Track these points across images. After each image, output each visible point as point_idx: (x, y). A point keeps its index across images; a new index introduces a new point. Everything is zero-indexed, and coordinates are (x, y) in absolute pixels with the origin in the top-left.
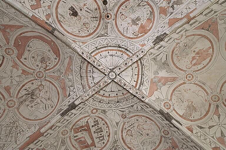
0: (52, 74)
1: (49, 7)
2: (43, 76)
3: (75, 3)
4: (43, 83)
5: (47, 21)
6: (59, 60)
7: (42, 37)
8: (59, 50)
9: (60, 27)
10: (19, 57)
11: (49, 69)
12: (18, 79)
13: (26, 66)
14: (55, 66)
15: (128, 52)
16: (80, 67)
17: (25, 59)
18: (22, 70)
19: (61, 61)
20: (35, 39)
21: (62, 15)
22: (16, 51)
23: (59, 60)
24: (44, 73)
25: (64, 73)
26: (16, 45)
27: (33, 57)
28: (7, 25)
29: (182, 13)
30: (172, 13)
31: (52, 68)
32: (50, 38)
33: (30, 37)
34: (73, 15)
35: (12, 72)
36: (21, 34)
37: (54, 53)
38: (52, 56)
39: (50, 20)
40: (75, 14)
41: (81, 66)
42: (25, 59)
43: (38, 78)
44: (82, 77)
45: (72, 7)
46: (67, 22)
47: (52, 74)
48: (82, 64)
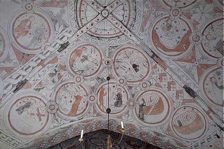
0: (163, 12)
1: (153, 73)
2: (173, 11)
3: (133, 74)
4: (174, 3)
5: (157, 64)
6: (154, 27)
7: (164, 50)
8: (152, 37)
9: (148, 58)
10: (190, 32)
11: (166, 18)
12: (197, 10)
13: (186, 23)
14: (160, 21)
15: (91, 34)
16: (135, 20)
17: (185, 30)
18: (191, 19)
19: (152, 25)
20: (171, 49)
21: (145, 66)
22: (191, 38)
23: (154, 27)
24: (171, 14)
25: (152, 13)
26: (188, 43)
27: (177, 31)
28: (189, 62)
29: (48, 68)
30: (56, 66)
31: (163, 19)
32: (158, 49)
33: (174, 51)
34: (136, 66)
35: (201, 19)
36: (180, 54)
37: (157, 35)
38: (160, 32)
39: (154, 64)
40: (135, 66)
41: (134, 21)
42: (185, 30)
43: (178, 9)
44: (135, 10)
45: (136, 72)
46: (142, 61)
47: (163, 12)
48: (133, 24)
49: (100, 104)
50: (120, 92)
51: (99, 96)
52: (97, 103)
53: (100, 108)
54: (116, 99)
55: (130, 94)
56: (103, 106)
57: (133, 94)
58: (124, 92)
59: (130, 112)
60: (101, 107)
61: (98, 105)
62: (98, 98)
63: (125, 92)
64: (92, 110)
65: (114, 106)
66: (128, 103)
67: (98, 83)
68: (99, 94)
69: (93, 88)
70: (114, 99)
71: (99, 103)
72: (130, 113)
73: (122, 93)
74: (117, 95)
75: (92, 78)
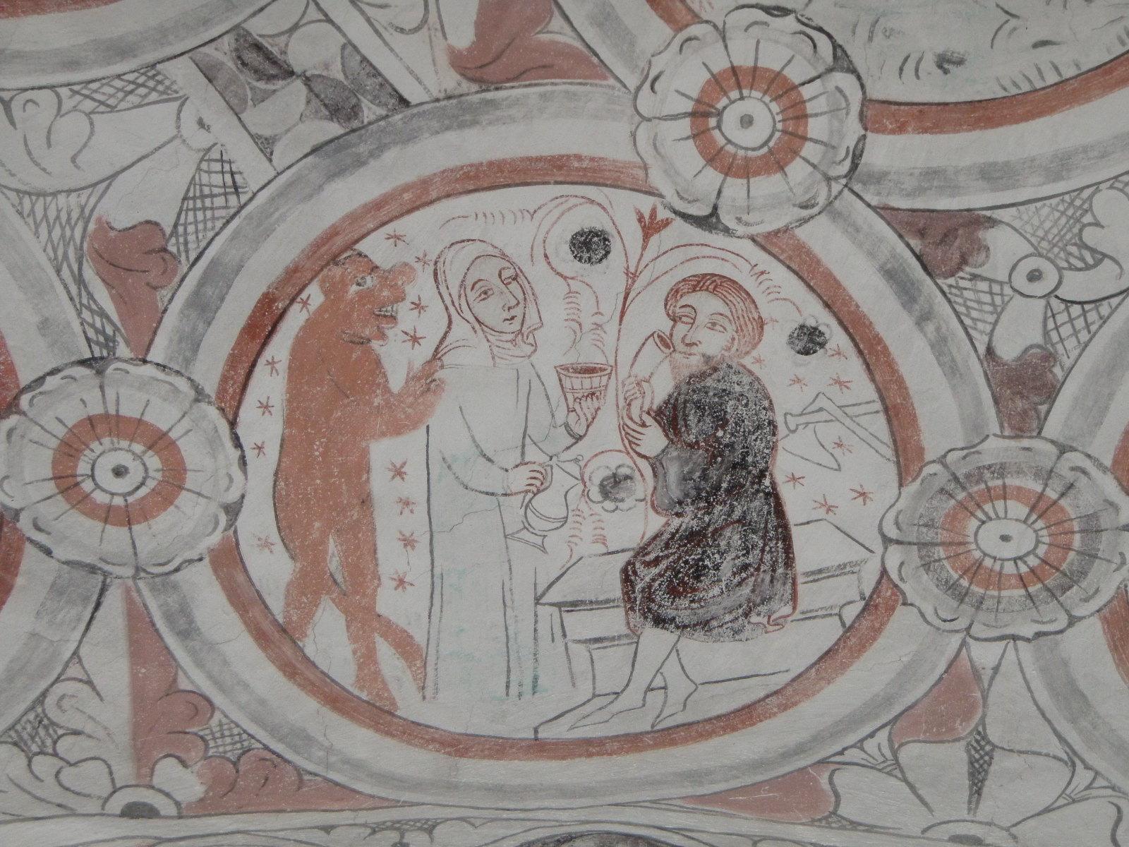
49: (310, 585)
50: (713, 344)
51: (263, 423)
52: (228, 560)
53: (300, 670)
54: (643, 485)
55: (953, 370)
56: (364, 620)
57: (1008, 351)
58: (809, 341)
59: (1006, 691)
60: (329, 640)
61: (244, 598)
62: (237, 470)
63: (837, 337)
64: (111, 666)
65: (614, 621)
66: (938, 542)
67: (253, 168)
68: (269, 384)
69: (134, 262)
70: (613, 485)
71: (271, 569)
72: (1010, 709)
73: (774, 363)
74: (671, 417)
75: (120, 50)
